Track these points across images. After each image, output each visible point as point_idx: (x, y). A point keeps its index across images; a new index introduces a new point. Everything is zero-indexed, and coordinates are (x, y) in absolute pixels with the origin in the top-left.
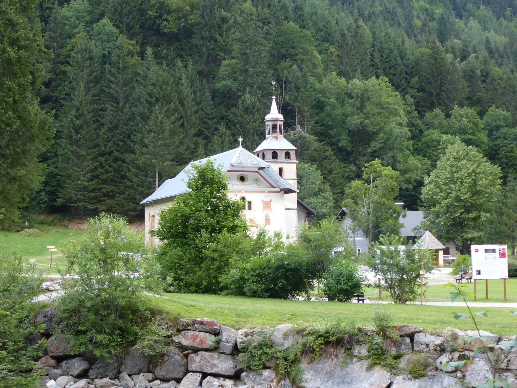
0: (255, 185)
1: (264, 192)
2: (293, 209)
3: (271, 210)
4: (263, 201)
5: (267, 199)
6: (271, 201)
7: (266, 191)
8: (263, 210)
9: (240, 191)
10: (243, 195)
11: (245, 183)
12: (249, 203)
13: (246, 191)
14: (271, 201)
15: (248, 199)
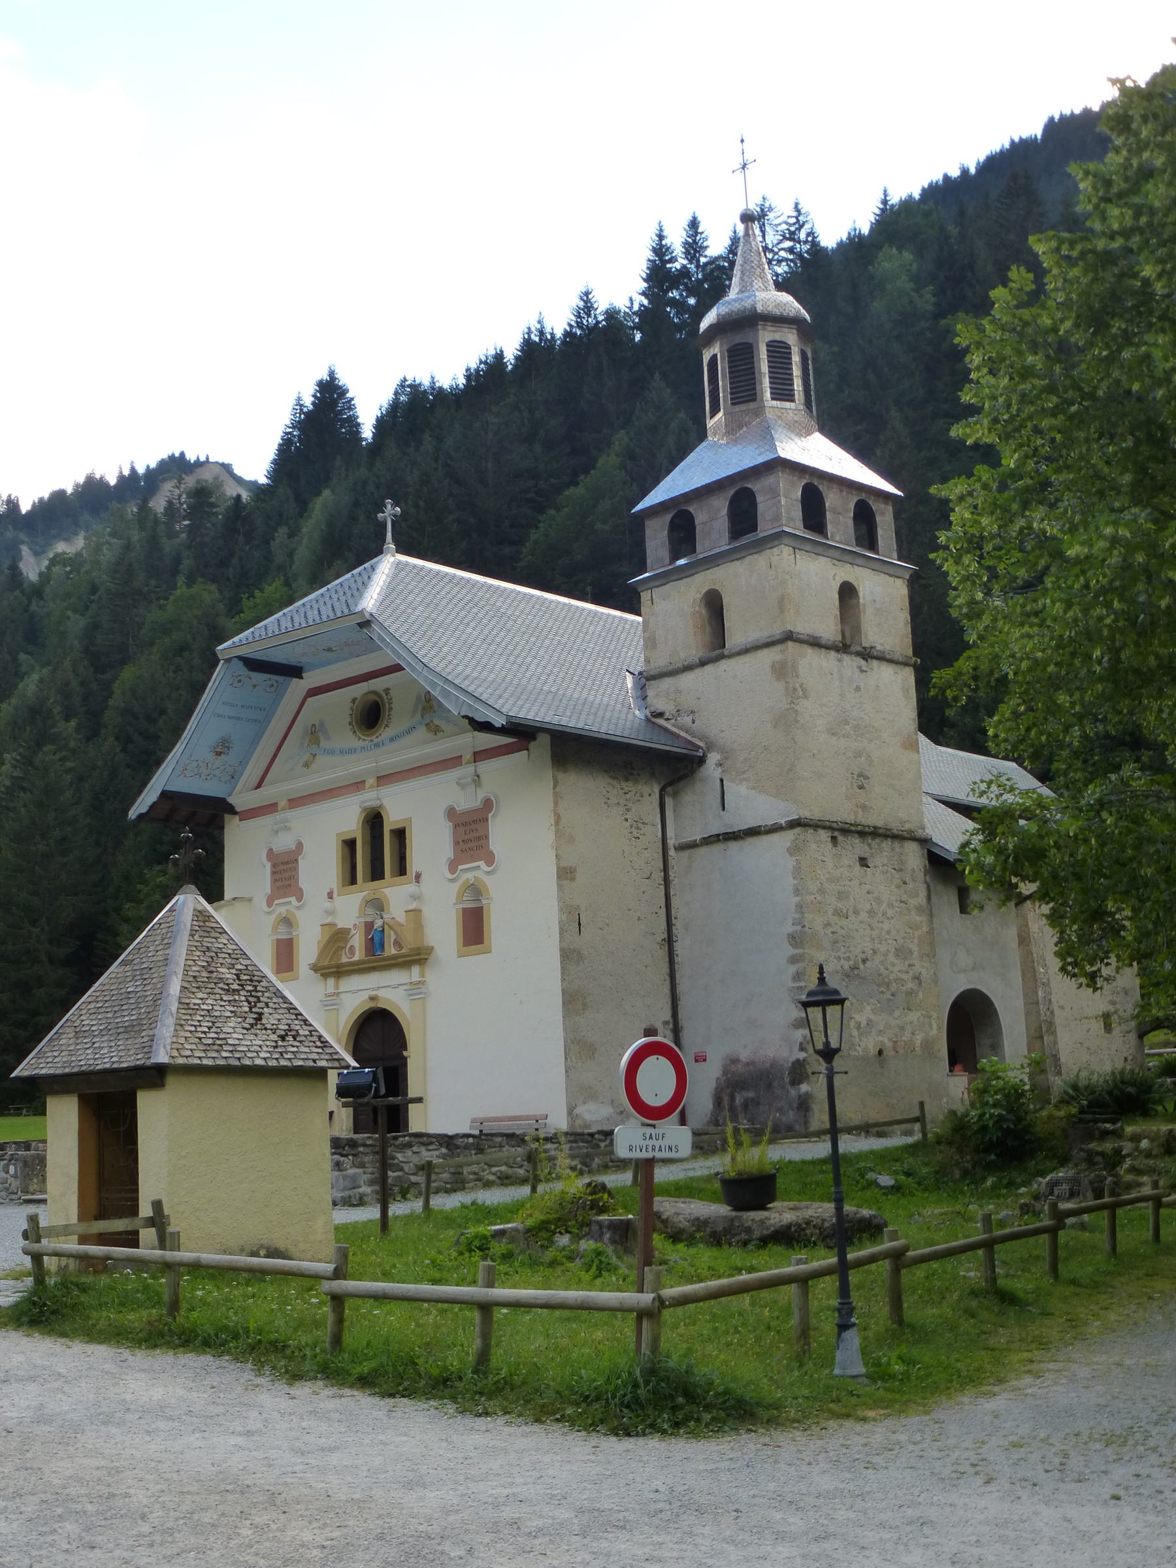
0: (422, 733)
1: (454, 762)
2: (775, 829)
3: (490, 859)
4: (451, 813)
5: (466, 802)
6: (488, 804)
7: (468, 756)
8: (453, 866)
9: (358, 786)
10: (369, 797)
11: (385, 733)
12: (400, 835)
13: (384, 779)
14: (488, 804)
15: (392, 819)
